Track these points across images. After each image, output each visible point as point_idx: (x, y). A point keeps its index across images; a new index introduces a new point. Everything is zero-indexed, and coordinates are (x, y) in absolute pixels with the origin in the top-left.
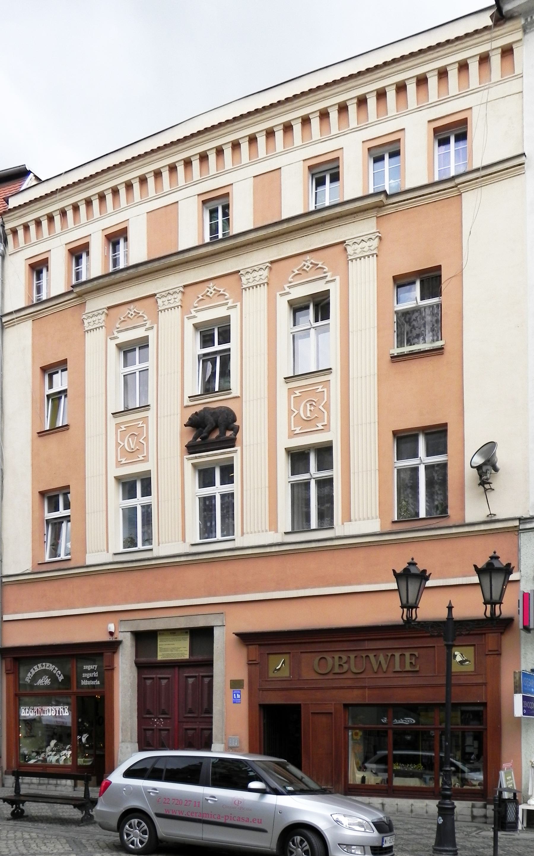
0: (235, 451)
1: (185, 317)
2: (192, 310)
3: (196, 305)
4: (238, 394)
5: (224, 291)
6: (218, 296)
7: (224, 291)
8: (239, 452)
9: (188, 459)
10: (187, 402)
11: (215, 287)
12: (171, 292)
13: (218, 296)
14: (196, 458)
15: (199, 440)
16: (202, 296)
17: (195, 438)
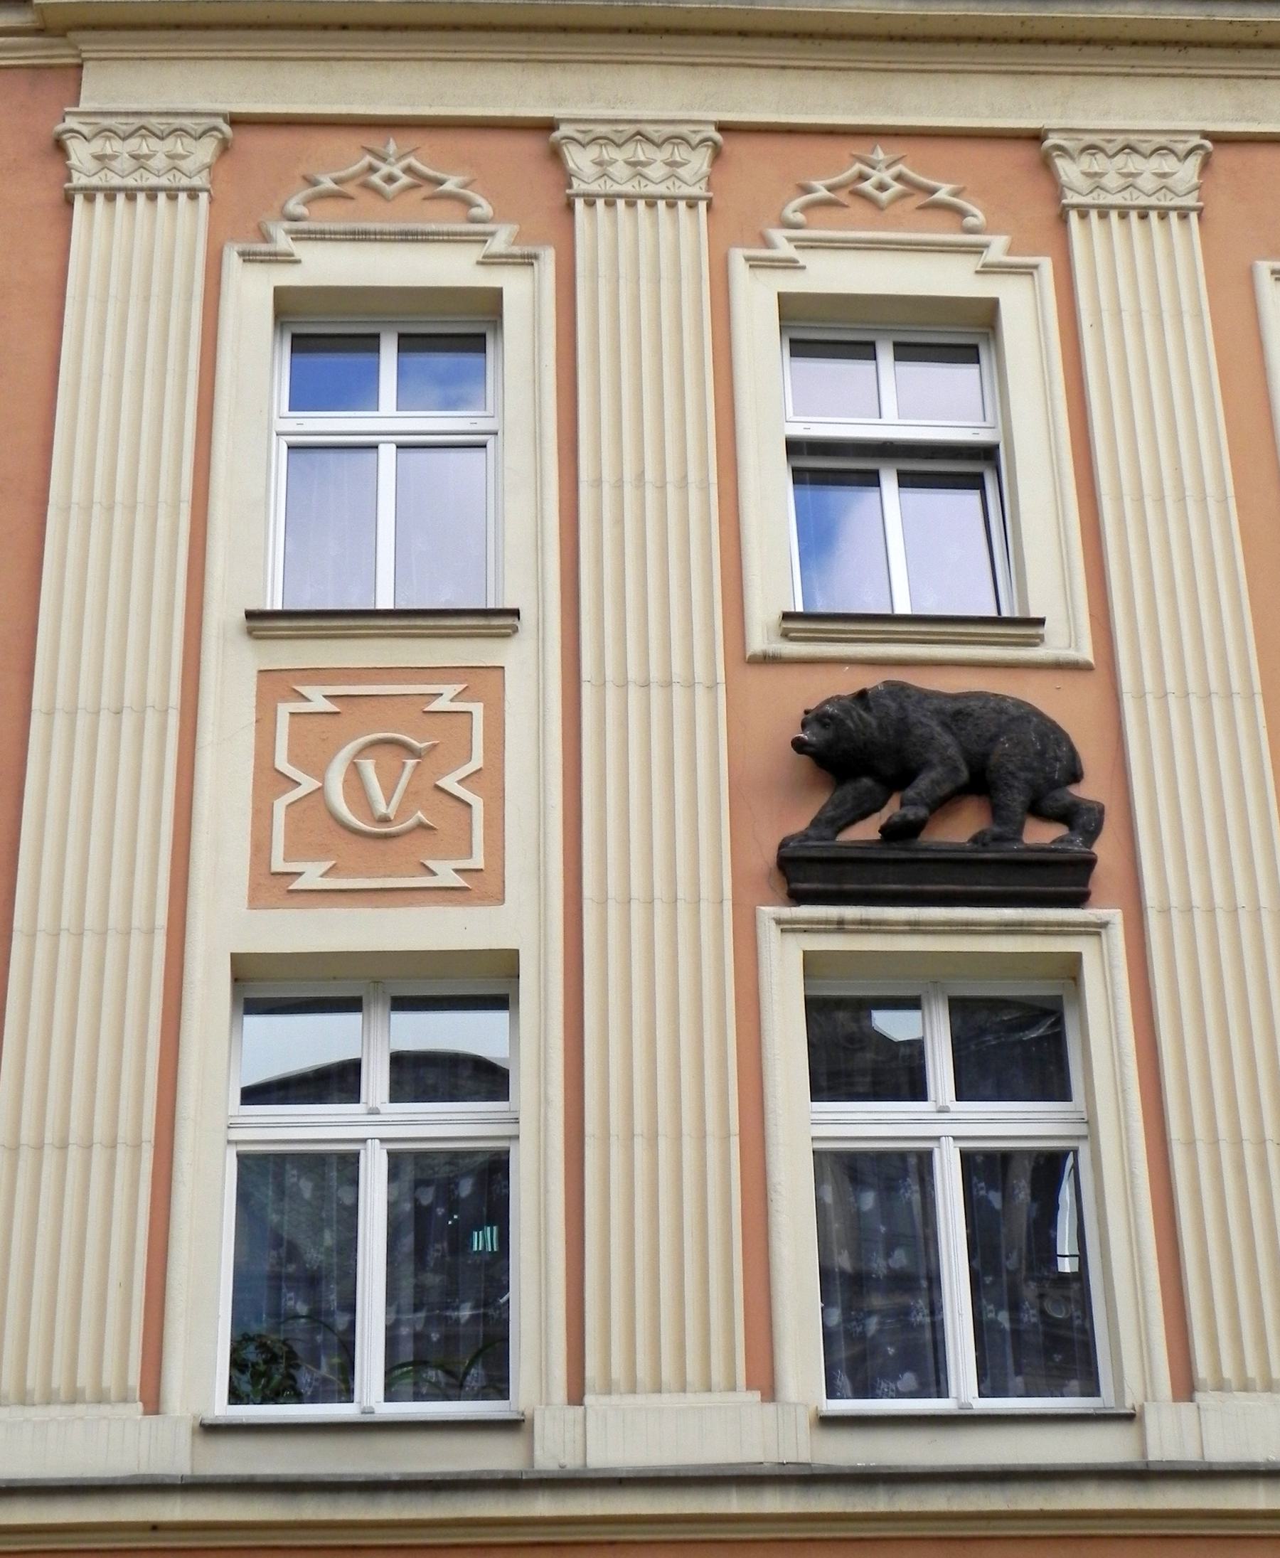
0: (1096, 930)
1: (738, 257)
2: (778, 235)
3: (800, 217)
4: (1086, 653)
5: (956, 194)
6: (921, 208)
7: (956, 194)
8: (1117, 936)
9: (786, 926)
10: (761, 639)
11: (900, 168)
12: (649, 129)
13: (921, 208)
14: (840, 926)
15: (866, 831)
16: (831, 189)
17: (833, 822)
